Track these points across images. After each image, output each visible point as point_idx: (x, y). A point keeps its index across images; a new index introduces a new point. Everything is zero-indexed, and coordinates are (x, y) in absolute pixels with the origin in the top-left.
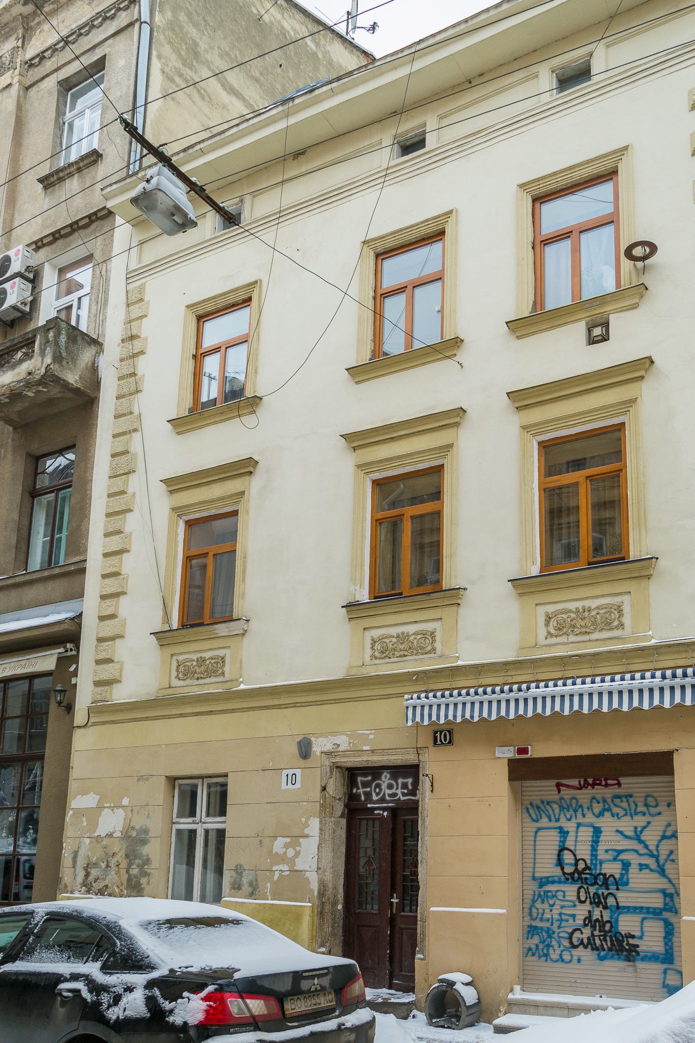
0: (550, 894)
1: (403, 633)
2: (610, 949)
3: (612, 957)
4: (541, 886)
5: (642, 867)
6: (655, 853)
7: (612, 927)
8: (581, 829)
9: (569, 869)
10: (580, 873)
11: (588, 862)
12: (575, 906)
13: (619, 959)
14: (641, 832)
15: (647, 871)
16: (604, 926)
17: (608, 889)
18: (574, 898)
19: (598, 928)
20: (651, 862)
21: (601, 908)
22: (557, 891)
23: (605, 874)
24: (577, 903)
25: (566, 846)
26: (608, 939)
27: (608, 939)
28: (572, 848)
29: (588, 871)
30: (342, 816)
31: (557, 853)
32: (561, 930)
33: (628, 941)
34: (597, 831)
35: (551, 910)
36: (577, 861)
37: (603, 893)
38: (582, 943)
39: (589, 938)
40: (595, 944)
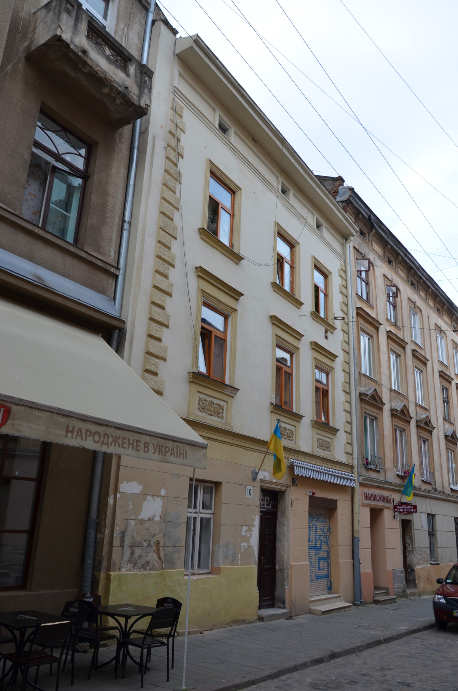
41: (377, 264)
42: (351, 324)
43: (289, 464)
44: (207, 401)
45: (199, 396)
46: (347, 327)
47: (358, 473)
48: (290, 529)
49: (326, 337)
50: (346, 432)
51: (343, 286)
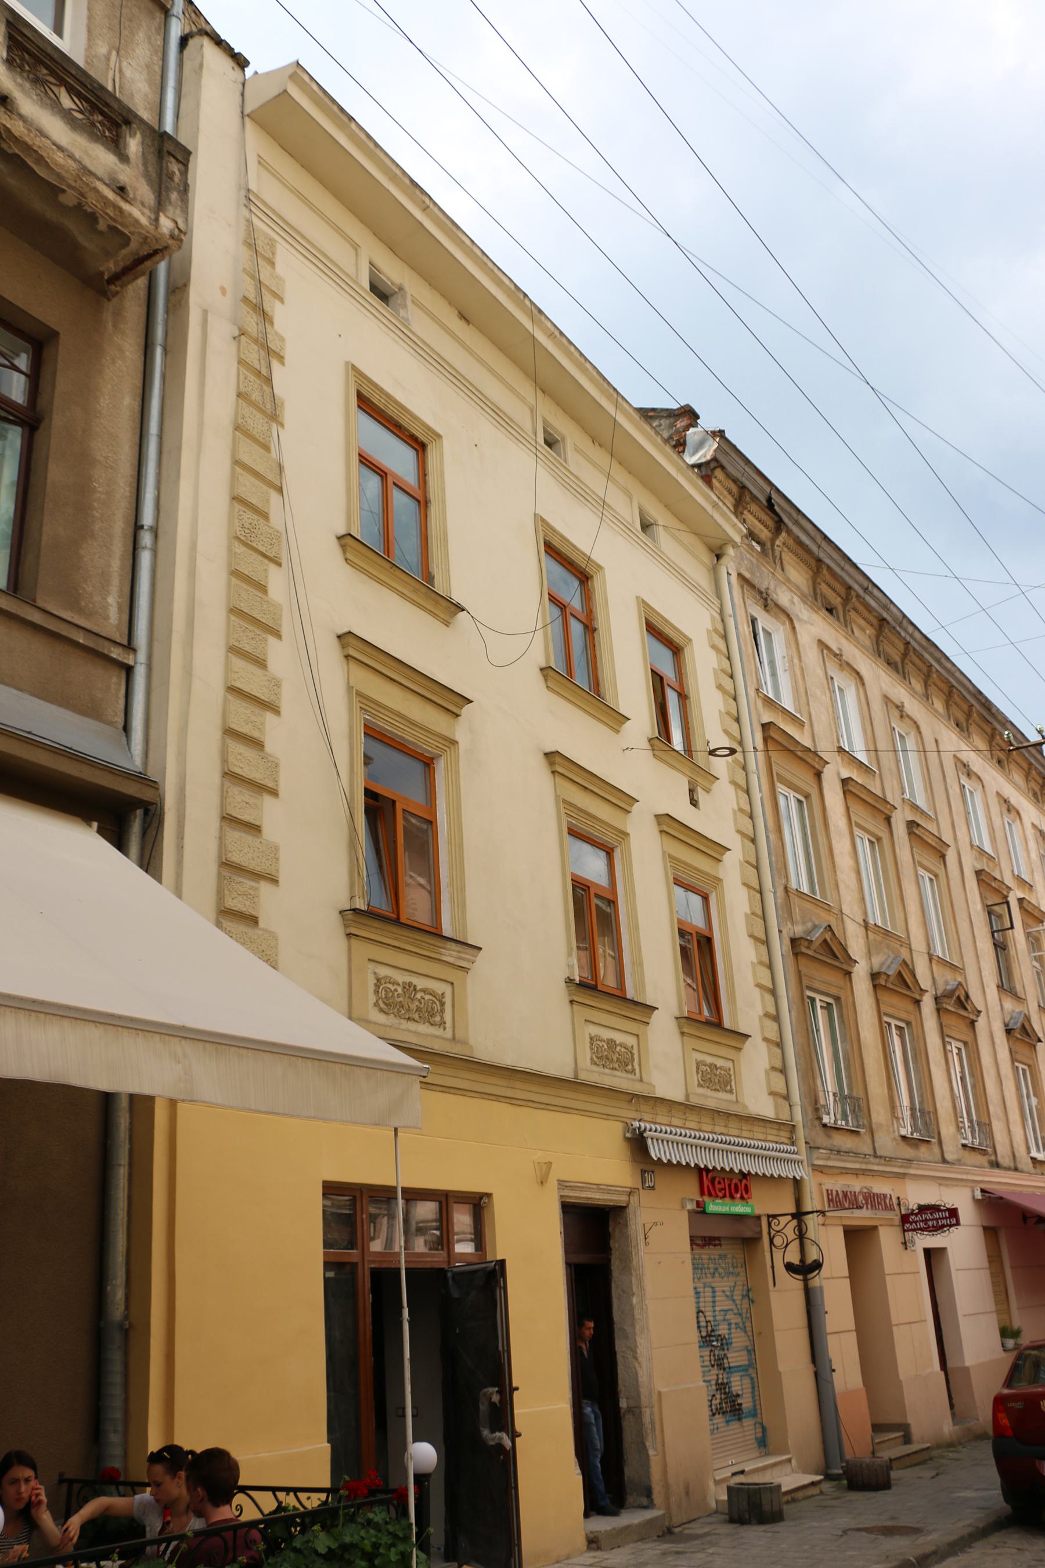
12: (710, 1371)
17: (723, 1350)
20: (739, 1320)
41: (799, 614)
42: (752, 765)
43: (628, 1135)
44: (399, 985)
45: (375, 973)
46: (744, 773)
47: (806, 1143)
48: (647, 1302)
49: (694, 803)
50: (765, 1039)
51: (723, 671)
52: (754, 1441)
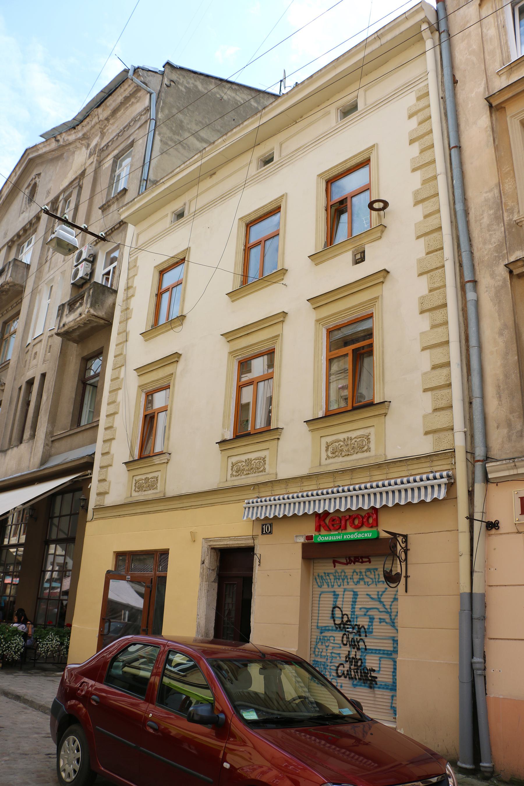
0: (326, 638)
1: (248, 459)
2: (360, 679)
3: (361, 685)
4: (321, 633)
5: (381, 620)
6: (389, 610)
7: (362, 663)
8: (346, 593)
9: (338, 621)
10: (344, 624)
11: (349, 616)
12: (340, 647)
13: (365, 686)
14: (382, 595)
15: (384, 624)
16: (357, 662)
17: (360, 635)
18: (340, 642)
19: (353, 664)
21: (356, 650)
22: (330, 637)
23: (359, 625)
24: (342, 646)
25: (337, 605)
26: (359, 671)
27: (359, 671)
28: (340, 606)
29: (349, 623)
30: (214, 581)
31: (331, 609)
32: (332, 664)
33: (371, 674)
34: (355, 594)
35: (327, 650)
36: (343, 615)
37: (357, 639)
38: (343, 674)
39: (347, 671)
40: (351, 675)
52: (389, 708)
